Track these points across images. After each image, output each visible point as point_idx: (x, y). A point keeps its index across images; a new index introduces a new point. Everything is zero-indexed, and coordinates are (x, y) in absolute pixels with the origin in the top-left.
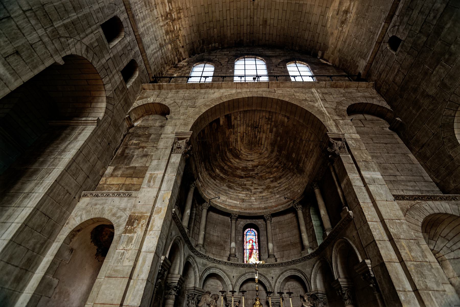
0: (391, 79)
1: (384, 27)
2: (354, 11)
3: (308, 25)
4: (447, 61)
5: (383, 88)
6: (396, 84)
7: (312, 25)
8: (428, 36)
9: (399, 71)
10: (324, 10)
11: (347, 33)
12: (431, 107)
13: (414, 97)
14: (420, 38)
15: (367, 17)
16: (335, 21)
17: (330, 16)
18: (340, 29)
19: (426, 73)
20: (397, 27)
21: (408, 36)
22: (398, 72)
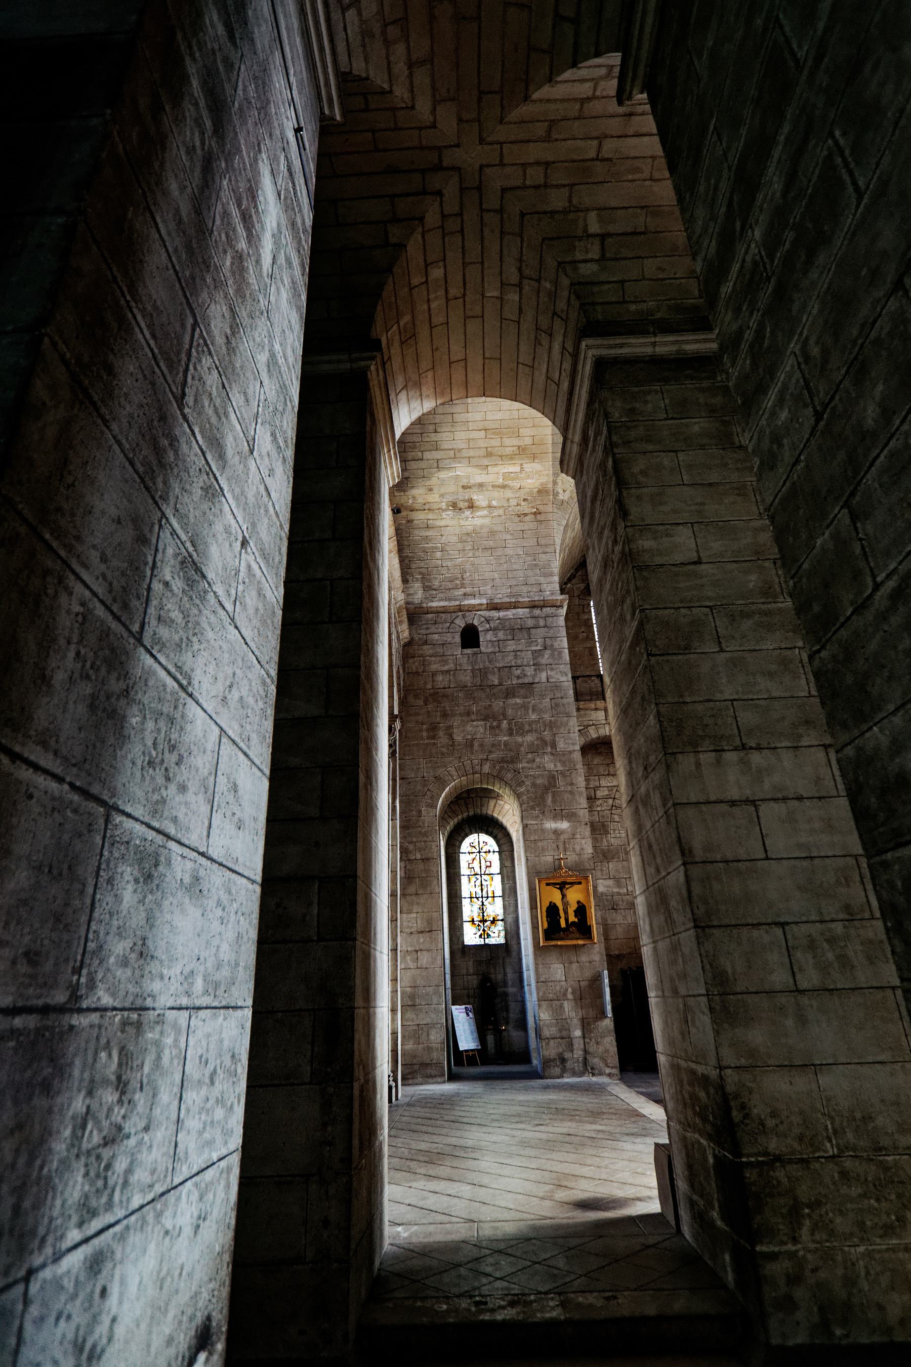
0: (434, 667)
1: (481, 605)
2: (478, 522)
3: (431, 427)
4: (492, 728)
5: (414, 663)
6: (433, 681)
7: (434, 437)
8: (501, 684)
9: (448, 671)
10: (465, 453)
11: (442, 523)
12: (444, 750)
13: (438, 719)
14: (494, 673)
15: (477, 554)
16: (452, 488)
17: (458, 473)
18: (444, 506)
19: (468, 714)
20: (488, 626)
21: (488, 654)
22: (447, 671)
